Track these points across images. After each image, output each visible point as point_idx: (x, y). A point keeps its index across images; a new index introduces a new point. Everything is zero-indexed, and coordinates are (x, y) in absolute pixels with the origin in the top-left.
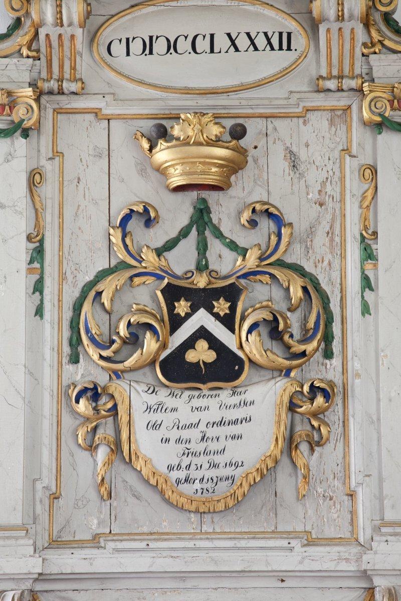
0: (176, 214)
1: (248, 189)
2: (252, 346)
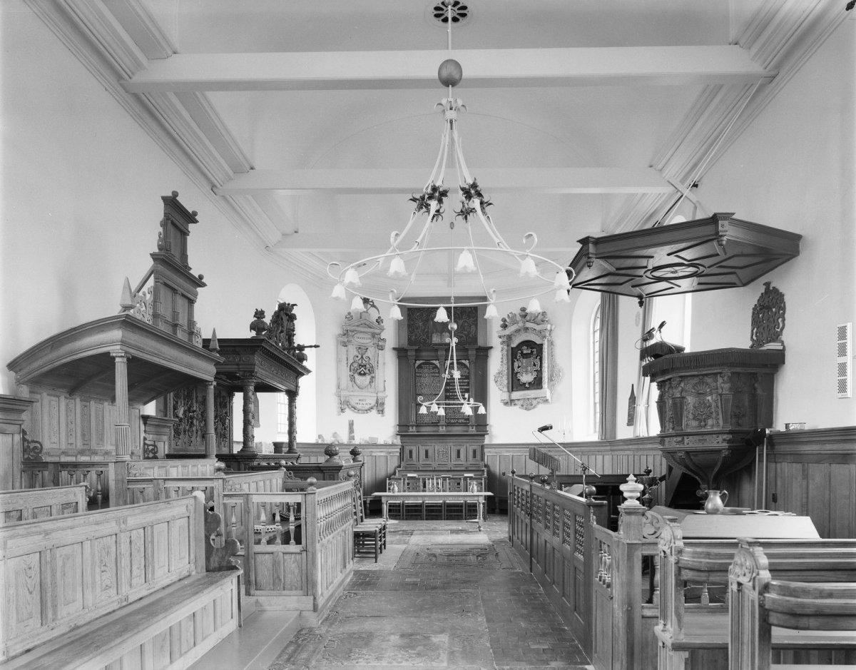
0: (360, 356)
1: (366, 355)
2: (367, 371)
